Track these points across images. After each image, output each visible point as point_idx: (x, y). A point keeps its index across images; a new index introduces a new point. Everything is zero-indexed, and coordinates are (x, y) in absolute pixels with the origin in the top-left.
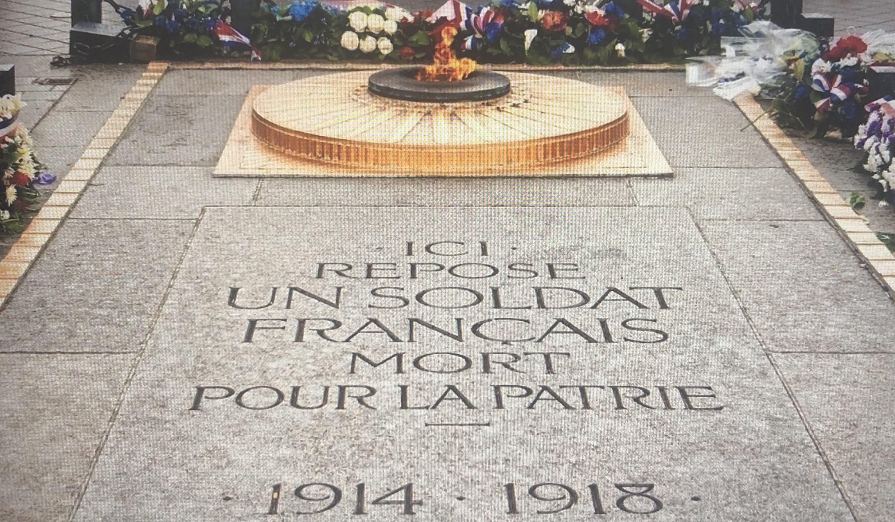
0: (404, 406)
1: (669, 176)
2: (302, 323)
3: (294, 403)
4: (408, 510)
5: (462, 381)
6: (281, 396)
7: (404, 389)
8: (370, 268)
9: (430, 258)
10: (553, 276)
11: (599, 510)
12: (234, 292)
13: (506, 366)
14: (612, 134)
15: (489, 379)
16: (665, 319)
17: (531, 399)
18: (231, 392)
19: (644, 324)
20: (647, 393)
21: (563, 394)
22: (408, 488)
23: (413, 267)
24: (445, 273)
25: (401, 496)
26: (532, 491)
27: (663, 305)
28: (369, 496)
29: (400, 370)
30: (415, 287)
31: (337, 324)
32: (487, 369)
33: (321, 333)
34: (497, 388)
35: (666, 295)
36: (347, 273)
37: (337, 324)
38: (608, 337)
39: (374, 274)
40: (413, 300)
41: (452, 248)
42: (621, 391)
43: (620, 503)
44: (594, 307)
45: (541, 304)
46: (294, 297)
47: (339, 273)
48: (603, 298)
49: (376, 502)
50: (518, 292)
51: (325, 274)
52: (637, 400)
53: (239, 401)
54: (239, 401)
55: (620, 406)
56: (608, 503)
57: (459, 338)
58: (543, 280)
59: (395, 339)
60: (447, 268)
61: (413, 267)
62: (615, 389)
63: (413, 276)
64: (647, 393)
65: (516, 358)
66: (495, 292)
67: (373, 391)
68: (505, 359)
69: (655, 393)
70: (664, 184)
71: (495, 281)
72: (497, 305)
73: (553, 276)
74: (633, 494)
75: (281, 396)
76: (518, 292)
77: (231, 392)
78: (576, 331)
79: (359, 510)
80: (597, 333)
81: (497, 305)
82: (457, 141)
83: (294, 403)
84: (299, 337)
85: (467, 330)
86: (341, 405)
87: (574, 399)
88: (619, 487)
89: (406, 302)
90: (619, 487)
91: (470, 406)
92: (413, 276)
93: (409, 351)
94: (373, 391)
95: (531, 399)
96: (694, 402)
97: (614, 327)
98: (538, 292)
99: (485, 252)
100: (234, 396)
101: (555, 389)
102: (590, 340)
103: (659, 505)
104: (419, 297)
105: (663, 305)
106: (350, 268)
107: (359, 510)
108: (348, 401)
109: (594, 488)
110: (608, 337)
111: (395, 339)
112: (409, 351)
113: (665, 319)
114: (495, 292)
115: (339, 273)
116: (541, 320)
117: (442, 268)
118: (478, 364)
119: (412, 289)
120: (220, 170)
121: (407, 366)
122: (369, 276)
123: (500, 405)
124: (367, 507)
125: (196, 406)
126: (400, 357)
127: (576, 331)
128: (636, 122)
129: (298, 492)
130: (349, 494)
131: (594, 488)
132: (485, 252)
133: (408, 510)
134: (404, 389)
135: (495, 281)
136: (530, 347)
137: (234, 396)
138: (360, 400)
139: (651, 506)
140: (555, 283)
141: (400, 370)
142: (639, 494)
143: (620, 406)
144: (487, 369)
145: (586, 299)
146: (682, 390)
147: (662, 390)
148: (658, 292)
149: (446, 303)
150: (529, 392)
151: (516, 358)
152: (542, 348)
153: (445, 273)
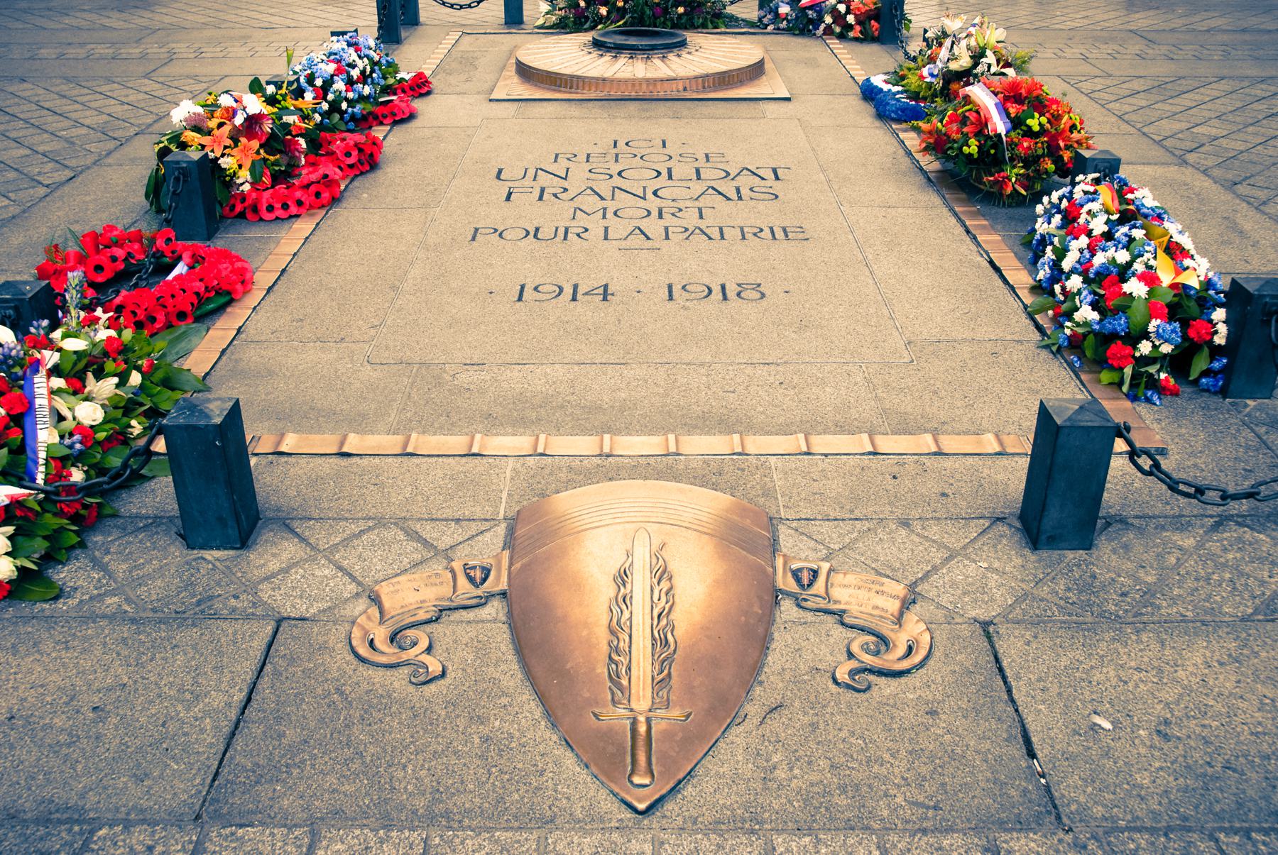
0: (606, 238)
1: (788, 99)
2: (543, 190)
3: (535, 236)
4: (605, 299)
5: (643, 224)
6: (528, 233)
7: (606, 229)
8: (588, 156)
10: (708, 160)
11: (725, 298)
12: (500, 171)
13: (673, 214)
15: (662, 223)
16: (778, 187)
17: (687, 234)
18: (496, 230)
19: (764, 190)
20: (761, 230)
21: (707, 231)
22: (606, 286)
23: (617, 155)
24: (638, 158)
25: (601, 290)
26: (684, 287)
27: (777, 178)
28: (581, 290)
29: (604, 217)
30: (619, 167)
31: (565, 190)
32: (661, 216)
33: (555, 195)
34: (666, 229)
35: (780, 172)
37: (565, 190)
38: (740, 198)
40: (615, 176)
41: (643, 144)
42: (746, 230)
43: (739, 295)
45: (699, 178)
49: (586, 294)
50: (683, 170)
52: (755, 234)
53: (500, 235)
54: (500, 235)
55: (744, 238)
56: (731, 293)
57: (644, 198)
58: (701, 163)
59: (602, 199)
61: (617, 155)
62: (742, 229)
63: (617, 161)
64: (761, 230)
65: (680, 210)
66: (669, 170)
67: (587, 230)
68: (673, 210)
69: (767, 231)
70: (786, 103)
71: (669, 164)
72: (670, 177)
73: (708, 160)
75: (528, 233)
76: (683, 170)
78: (720, 193)
79: (574, 299)
80: (734, 196)
81: (670, 177)
82: (649, 75)
83: (535, 236)
84: (541, 198)
85: (650, 195)
86: (565, 238)
87: (715, 233)
88: (739, 285)
90: (739, 285)
91: (648, 238)
92: (617, 161)
93: (611, 206)
94: (587, 230)
95: (687, 234)
96: (790, 235)
97: (745, 192)
98: (698, 171)
99: (664, 146)
101: (703, 228)
102: (729, 199)
103: (763, 296)
104: (620, 174)
105: (777, 178)
107: (574, 299)
108: (570, 235)
109: (723, 287)
110: (740, 198)
111: (602, 199)
112: (611, 206)
113: (778, 187)
114: (669, 170)
116: (698, 188)
118: (655, 213)
119: (615, 168)
121: (610, 215)
123: (667, 237)
124: (579, 297)
125: (473, 239)
126: (605, 209)
127: (720, 193)
129: (536, 289)
130: (568, 291)
131: (723, 287)
132: (664, 146)
133: (605, 299)
134: (606, 229)
135: (669, 164)
136: (688, 203)
138: (578, 235)
139: (759, 295)
140: (709, 165)
141: (604, 217)
143: (744, 238)
144: (661, 216)
145: (728, 174)
146: (784, 230)
147: (772, 229)
148: (775, 171)
149: (639, 178)
150: (687, 230)
151: (680, 210)
152: (697, 204)
153: (638, 158)
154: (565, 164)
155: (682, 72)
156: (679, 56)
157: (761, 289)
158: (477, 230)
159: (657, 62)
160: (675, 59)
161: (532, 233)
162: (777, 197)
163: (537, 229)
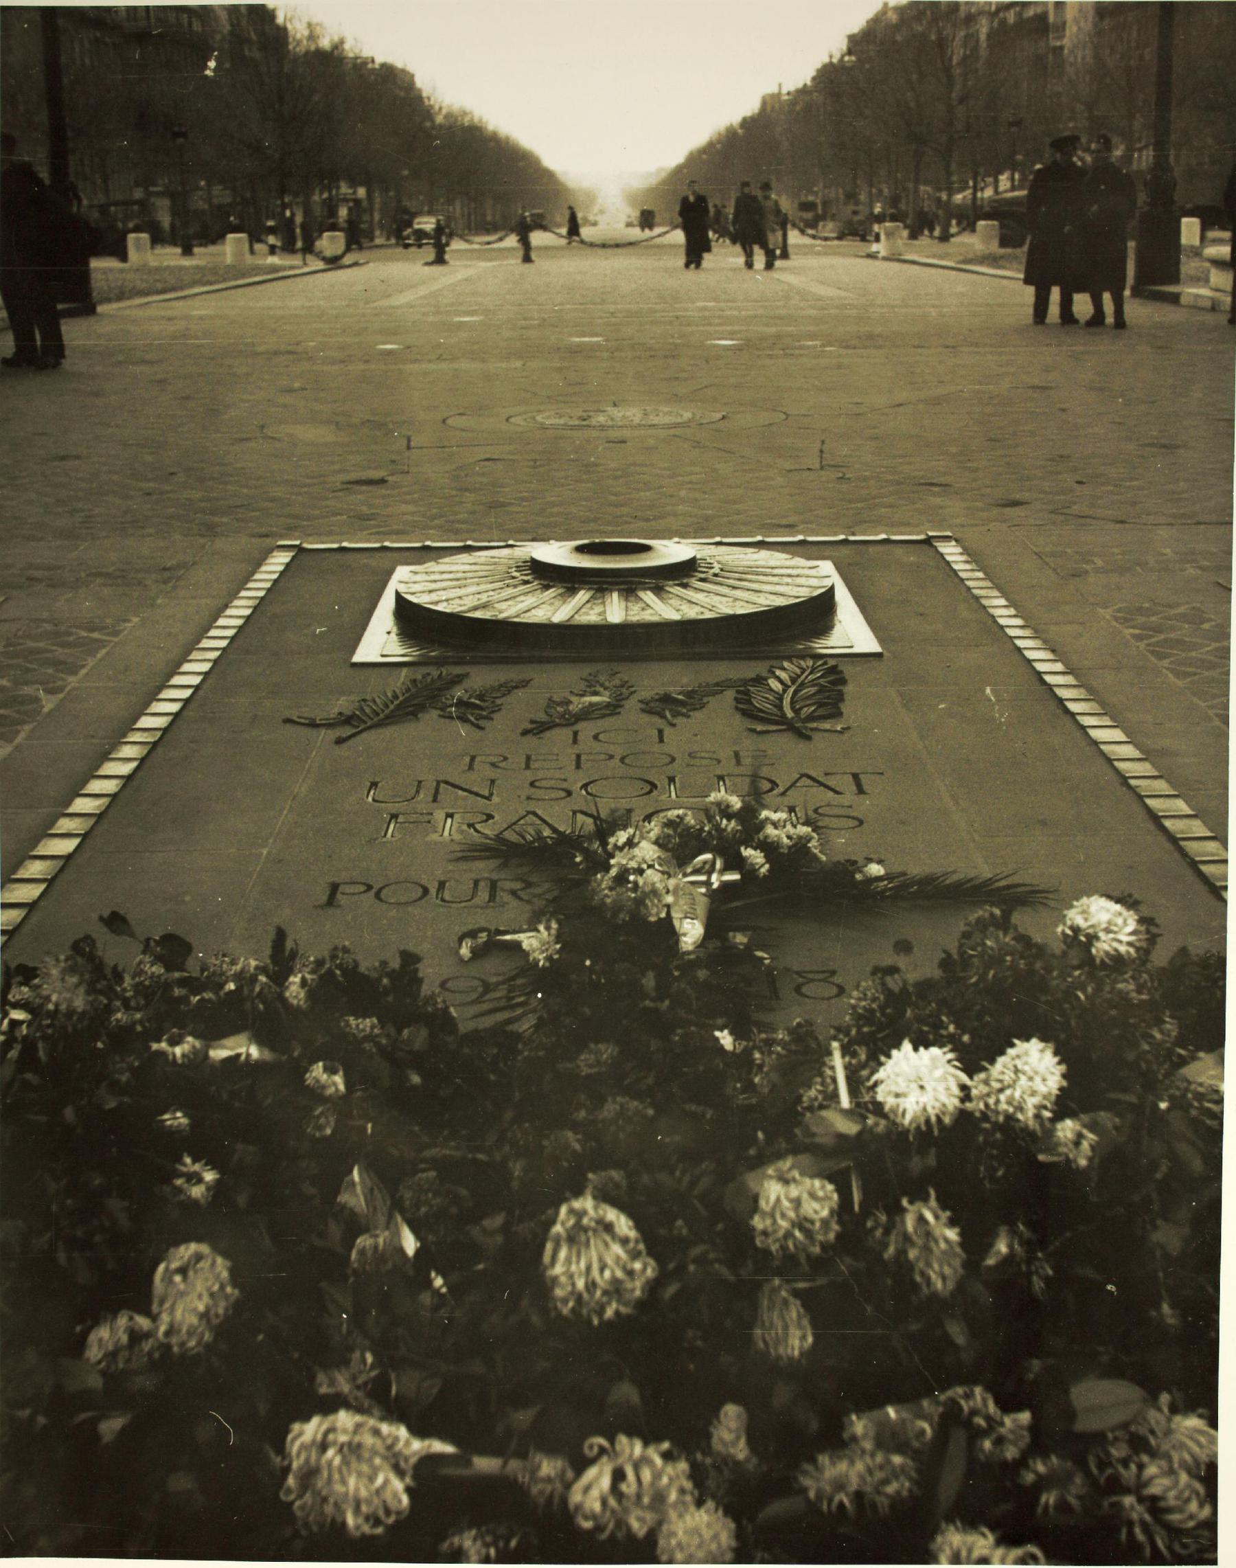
9: (597, 746)
14: (818, 612)
18: (370, 887)
23: (578, 757)
36: (503, 765)
39: (534, 765)
44: (783, 794)
46: (441, 790)
47: (493, 765)
48: (793, 785)
51: (476, 765)
53: (378, 896)
54: (378, 896)
60: (618, 757)
61: (578, 757)
70: (875, 663)
71: (669, 770)
74: (813, 980)
77: (370, 887)
89: (569, 793)
92: (578, 766)
100: (374, 891)
106: (505, 759)
108: (499, 893)
115: (493, 765)
117: (611, 757)
120: (357, 658)
122: (528, 767)
128: (843, 597)
137: (374, 891)
142: (820, 980)
148: (856, 777)
153: (616, 761)
154: (491, 773)
155: (692, 613)
156: (685, 586)
157: (838, 979)
158: (334, 888)
159: (648, 596)
160: (678, 590)
161: (433, 891)
162: (861, 822)
163: (442, 885)
